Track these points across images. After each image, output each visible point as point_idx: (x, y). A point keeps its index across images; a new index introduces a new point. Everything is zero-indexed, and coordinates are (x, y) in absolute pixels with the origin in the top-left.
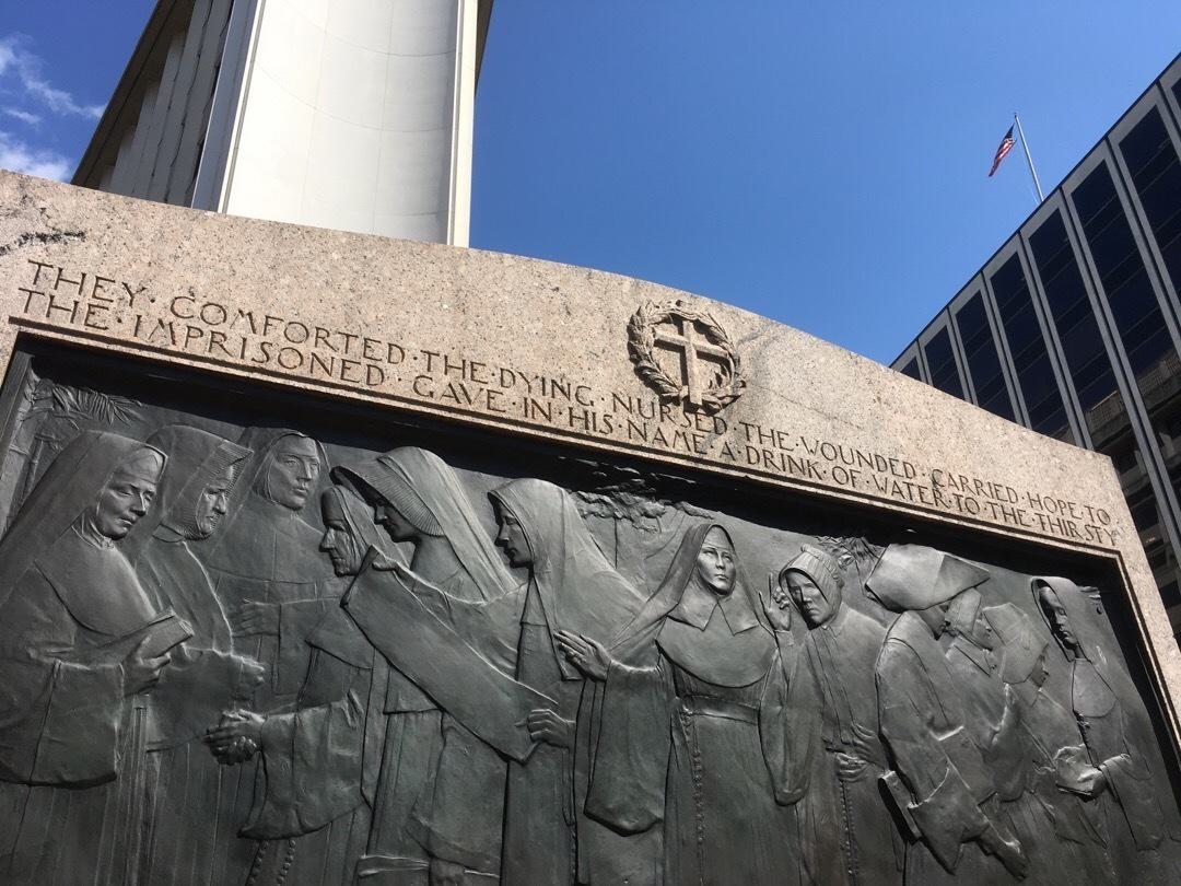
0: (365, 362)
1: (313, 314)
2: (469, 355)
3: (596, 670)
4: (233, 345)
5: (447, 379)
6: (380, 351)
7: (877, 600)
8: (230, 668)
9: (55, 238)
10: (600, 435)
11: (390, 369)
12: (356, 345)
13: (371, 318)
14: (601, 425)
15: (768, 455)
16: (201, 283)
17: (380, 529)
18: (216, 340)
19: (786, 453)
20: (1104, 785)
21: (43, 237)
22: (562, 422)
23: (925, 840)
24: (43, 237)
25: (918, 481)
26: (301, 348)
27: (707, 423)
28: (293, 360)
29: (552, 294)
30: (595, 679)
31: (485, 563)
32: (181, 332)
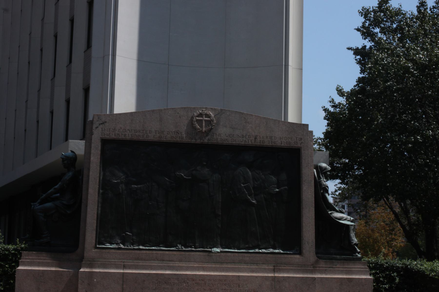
0: (146, 134)
5: (158, 135)
10: (184, 140)
15: (217, 139)
18: (125, 135)
21: (101, 124)
24: (101, 124)
26: (136, 134)
32: (120, 135)
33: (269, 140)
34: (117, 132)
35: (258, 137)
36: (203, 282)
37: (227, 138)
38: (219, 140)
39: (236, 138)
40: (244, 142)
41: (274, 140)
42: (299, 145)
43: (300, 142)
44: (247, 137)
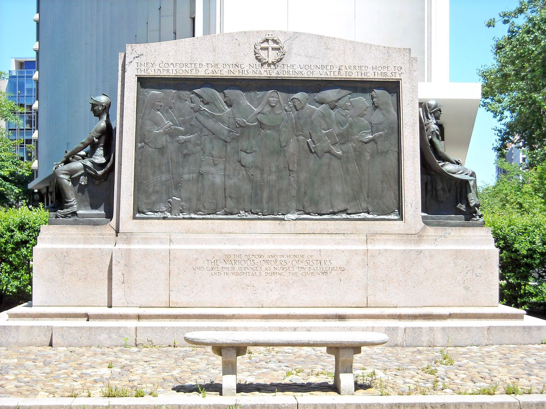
0: (195, 69)
1: (184, 61)
3: (243, 125)
4: (171, 71)
7: (317, 102)
8: (178, 130)
9: (138, 57)
10: (246, 75)
11: (200, 70)
12: (193, 65)
13: (195, 59)
14: (246, 73)
15: (289, 72)
17: (201, 102)
18: (168, 71)
19: (294, 70)
21: (137, 57)
23: (315, 152)
28: (181, 72)
29: (235, 41)
30: (243, 127)
31: (222, 106)
32: (162, 71)
33: (358, 71)
35: (343, 68)
36: (274, 259)
37: (301, 70)
38: (291, 73)
39: (313, 70)
40: (324, 74)
41: (365, 71)
42: (398, 77)
43: (400, 73)
44: (329, 68)
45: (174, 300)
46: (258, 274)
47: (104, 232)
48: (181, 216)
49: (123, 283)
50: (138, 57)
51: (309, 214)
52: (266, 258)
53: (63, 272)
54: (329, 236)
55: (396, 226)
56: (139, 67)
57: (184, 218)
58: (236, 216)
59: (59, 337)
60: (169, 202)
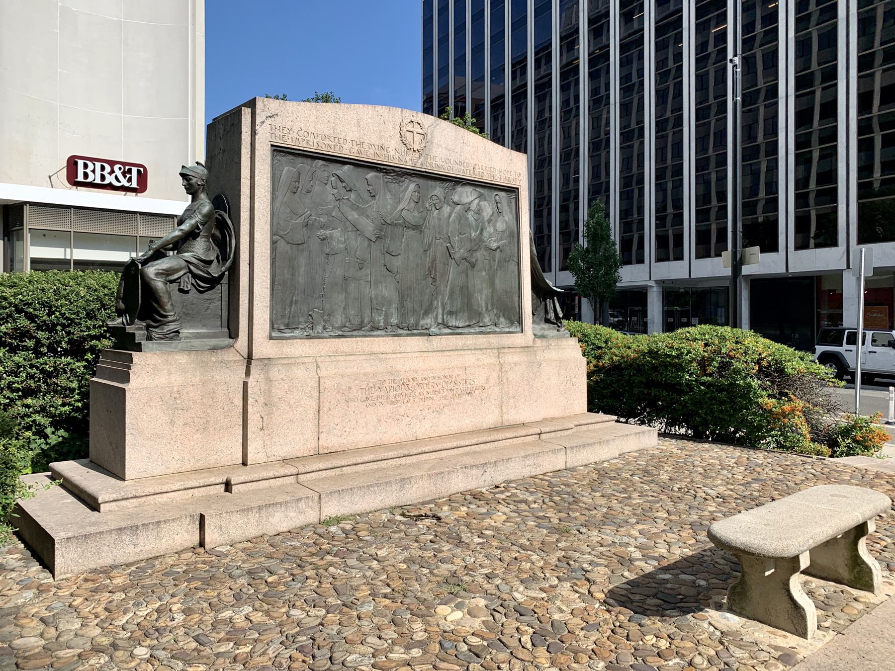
2: (362, 140)
4: (311, 143)
5: (357, 148)
6: (342, 142)
9: (272, 116)
11: (345, 147)
12: (336, 139)
16: (302, 125)
20: (498, 247)
22: (383, 158)
25: (470, 168)
27: (417, 155)
34: (295, 135)
35: (477, 167)
37: (443, 164)
45: (325, 444)
46: (412, 401)
47: (226, 358)
48: (326, 334)
49: (262, 429)
50: (272, 116)
51: (448, 327)
52: (420, 381)
53: (172, 423)
54: (469, 352)
55: (518, 339)
56: (273, 131)
57: (331, 337)
58: (383, 333)
59: (215, 530)
60: (310, 315)
